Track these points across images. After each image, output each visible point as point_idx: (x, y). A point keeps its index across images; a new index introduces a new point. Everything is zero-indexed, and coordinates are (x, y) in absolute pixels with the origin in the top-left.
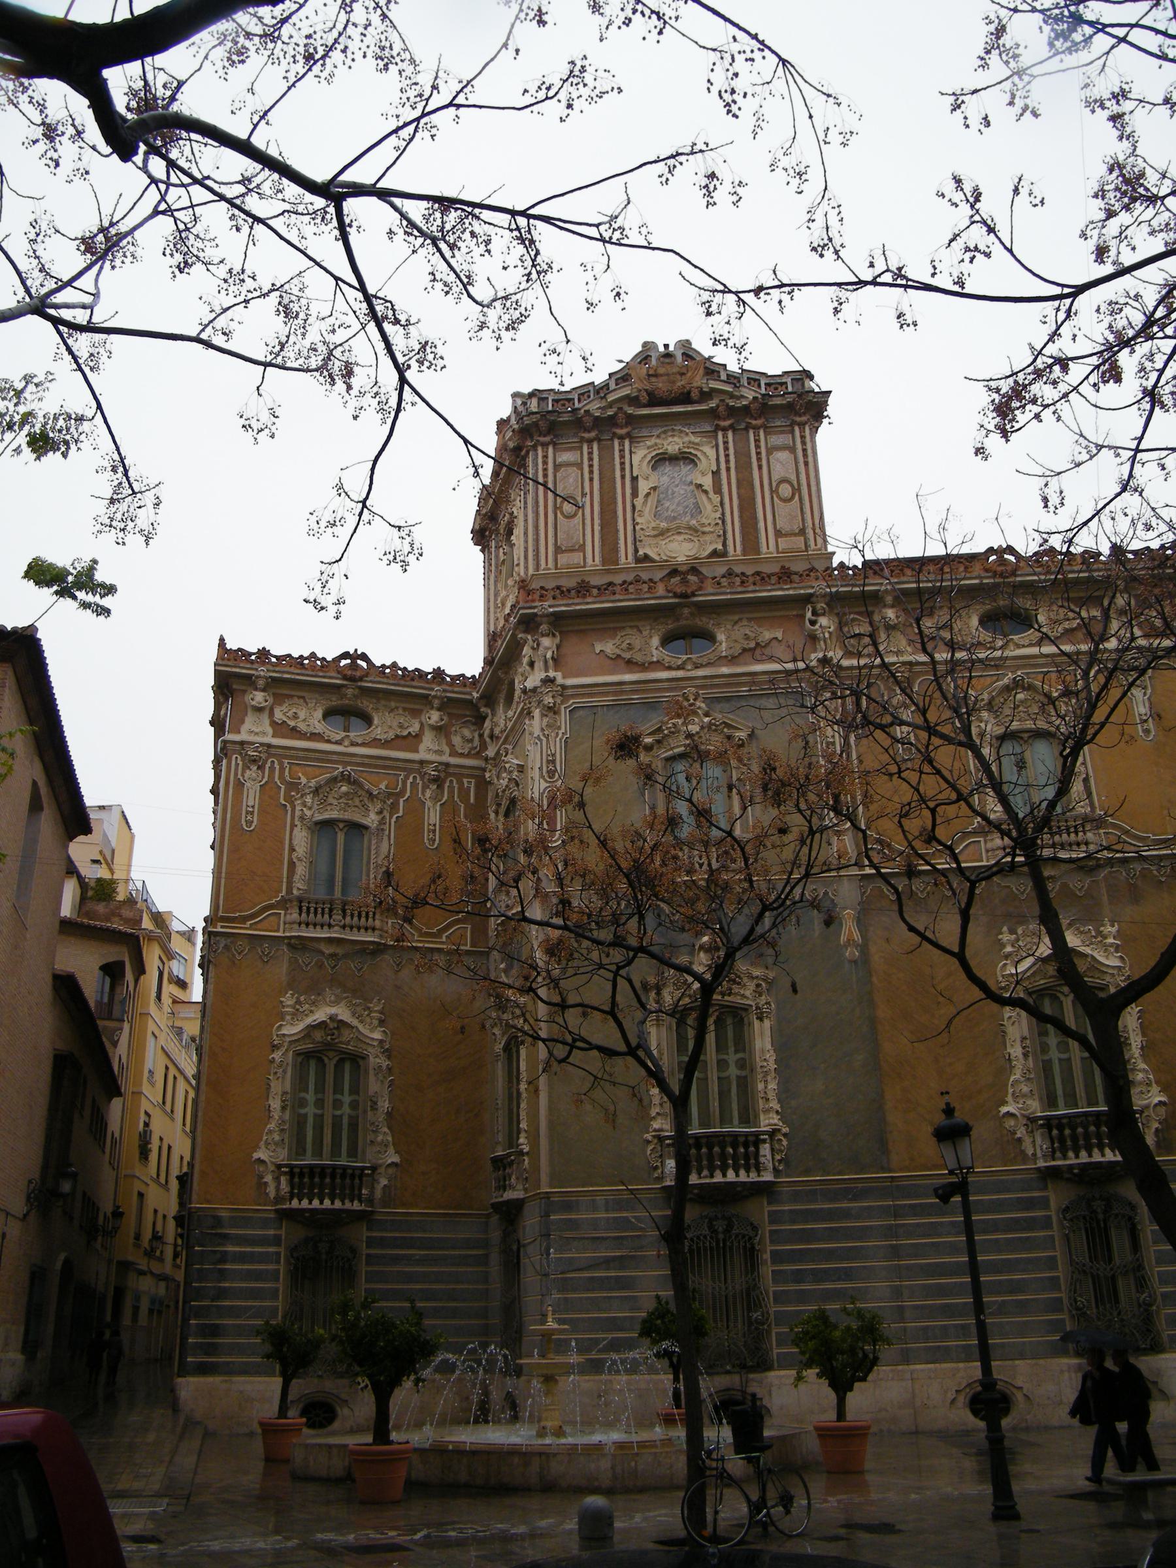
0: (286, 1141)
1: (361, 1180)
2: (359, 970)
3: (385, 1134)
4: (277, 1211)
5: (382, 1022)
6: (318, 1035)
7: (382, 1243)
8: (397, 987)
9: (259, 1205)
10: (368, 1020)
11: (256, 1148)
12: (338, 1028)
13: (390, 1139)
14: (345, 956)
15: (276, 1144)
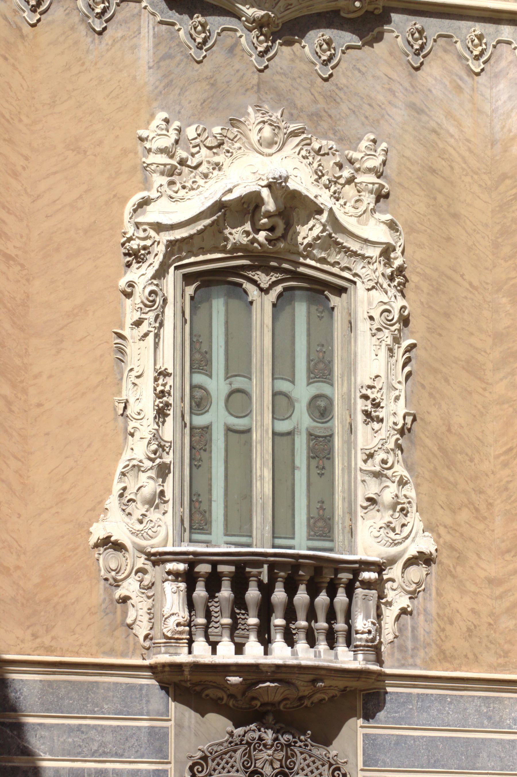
0: (169, 495)
5: (381, 196)
11: (98, 510)
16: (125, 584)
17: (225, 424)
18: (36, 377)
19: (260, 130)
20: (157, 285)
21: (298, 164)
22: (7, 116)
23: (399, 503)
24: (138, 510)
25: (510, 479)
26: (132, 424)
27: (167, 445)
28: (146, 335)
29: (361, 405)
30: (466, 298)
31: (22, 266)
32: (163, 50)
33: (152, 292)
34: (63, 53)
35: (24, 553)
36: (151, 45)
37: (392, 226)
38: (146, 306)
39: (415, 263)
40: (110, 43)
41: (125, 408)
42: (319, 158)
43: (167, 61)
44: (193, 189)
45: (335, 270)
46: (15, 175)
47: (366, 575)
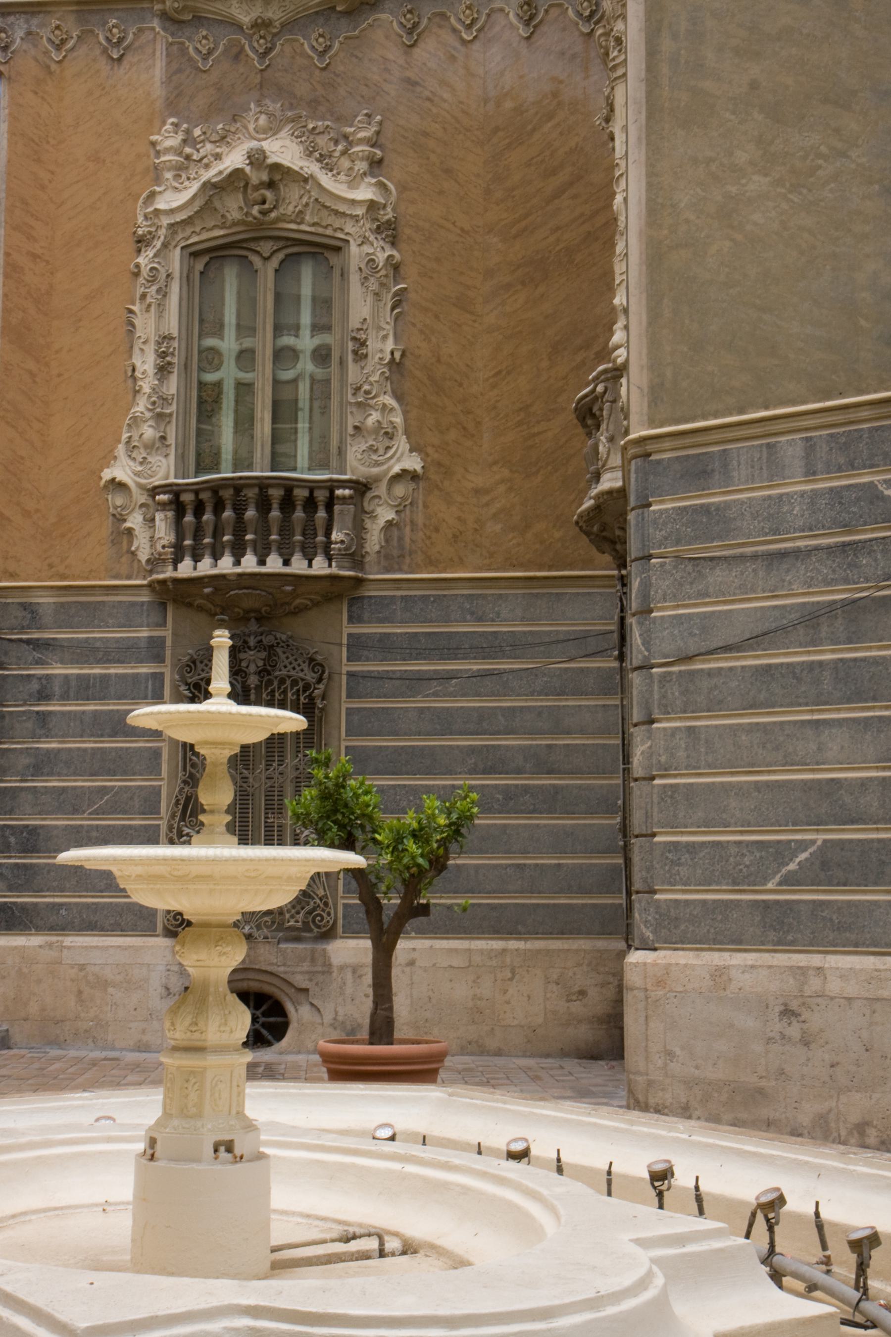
0: (171, 440)
1: (329, 507)
2: (322, 54)
3: (387, 412)
4: (150, 585)
5: (376, 164)
6: (233, 207)
7: (386, 647)
8: (411, 83)
9: (117, 577)
10: (345, 163)
11: (109, 458)
12: (271, 185)
13: (398, 419)
14: (288, 26)
15: (150, 447)
16: (131, 518)
17: (236, 379)
18: (57, 352)
19: (257, 120)
20: (159, 263)
21: (287, 142)
22: (37, 140)
23: (382, 428)
24: (139, 455)
25: (498, 398)
26: (140, 383)
27: (170, 397)
28: (149, 306)
29: (351, 345)
30: (457, 242)
31: (48, 262)
32: (175, 66)
33: (152, 269)
34: (86, 81)
35: (44, 498)
36: (164, 64)
37: (382, 186)
38: (148, 281)
39: (408, 217)
40: (127, 67)
41: (134, 370)
42: (312, 137)
43: (178, 75)
44: (195, 179)
45: (329, 232)
46: (43, 188)
47: (339, 492)
